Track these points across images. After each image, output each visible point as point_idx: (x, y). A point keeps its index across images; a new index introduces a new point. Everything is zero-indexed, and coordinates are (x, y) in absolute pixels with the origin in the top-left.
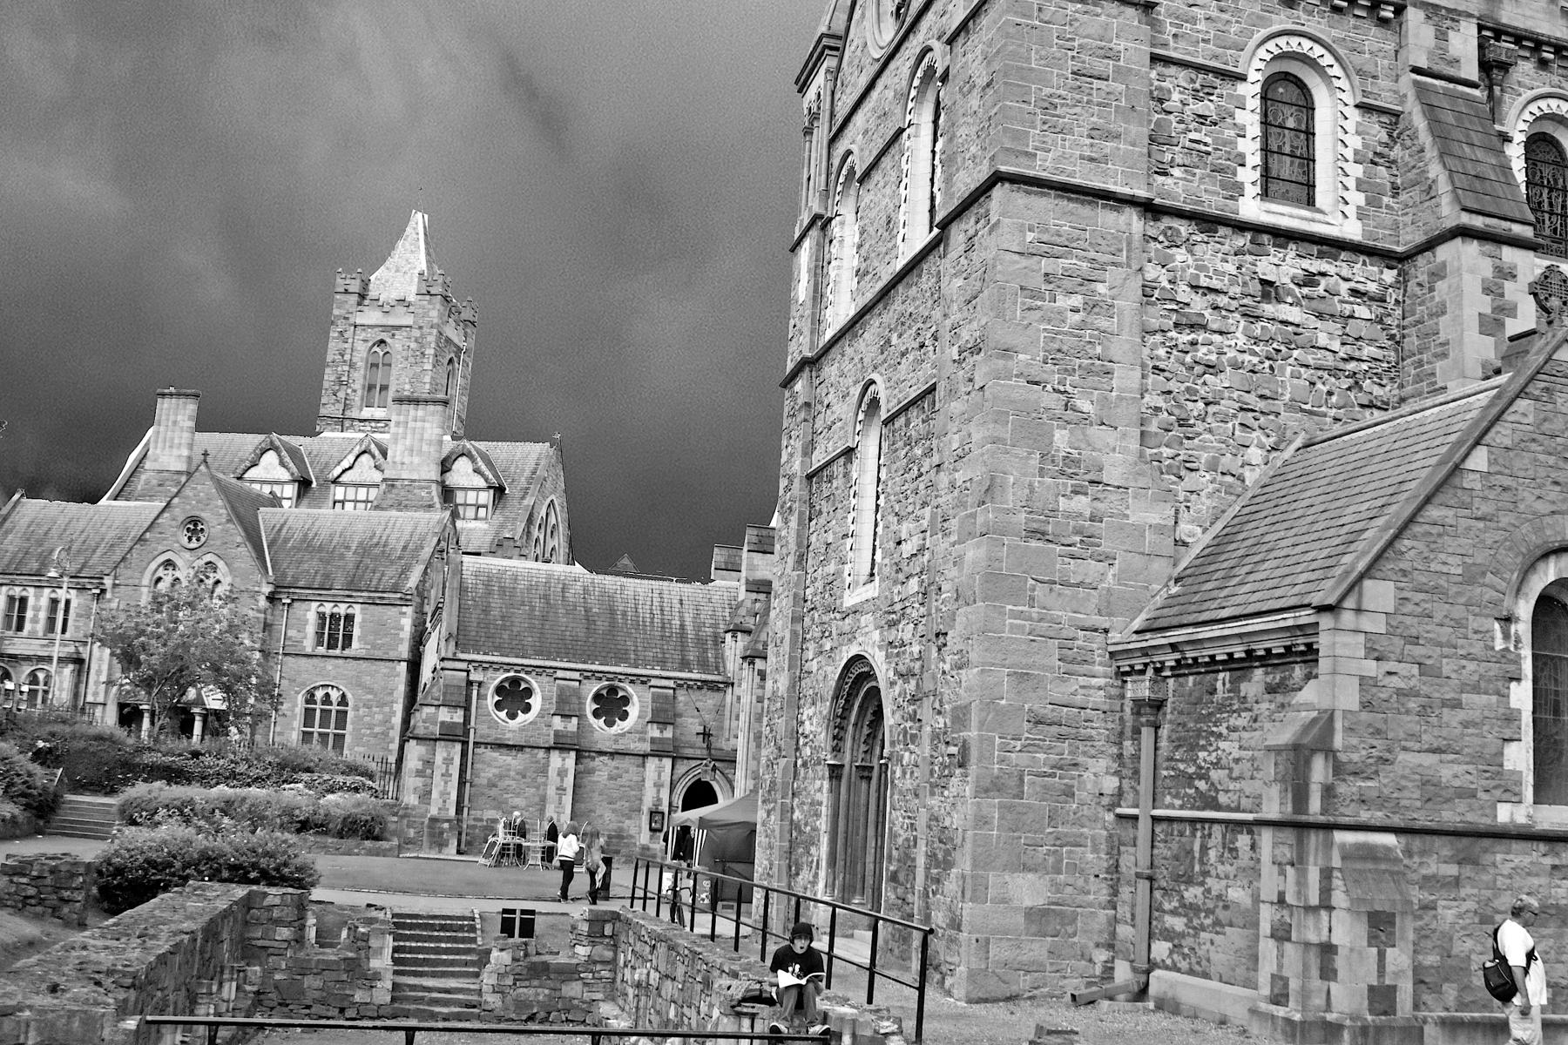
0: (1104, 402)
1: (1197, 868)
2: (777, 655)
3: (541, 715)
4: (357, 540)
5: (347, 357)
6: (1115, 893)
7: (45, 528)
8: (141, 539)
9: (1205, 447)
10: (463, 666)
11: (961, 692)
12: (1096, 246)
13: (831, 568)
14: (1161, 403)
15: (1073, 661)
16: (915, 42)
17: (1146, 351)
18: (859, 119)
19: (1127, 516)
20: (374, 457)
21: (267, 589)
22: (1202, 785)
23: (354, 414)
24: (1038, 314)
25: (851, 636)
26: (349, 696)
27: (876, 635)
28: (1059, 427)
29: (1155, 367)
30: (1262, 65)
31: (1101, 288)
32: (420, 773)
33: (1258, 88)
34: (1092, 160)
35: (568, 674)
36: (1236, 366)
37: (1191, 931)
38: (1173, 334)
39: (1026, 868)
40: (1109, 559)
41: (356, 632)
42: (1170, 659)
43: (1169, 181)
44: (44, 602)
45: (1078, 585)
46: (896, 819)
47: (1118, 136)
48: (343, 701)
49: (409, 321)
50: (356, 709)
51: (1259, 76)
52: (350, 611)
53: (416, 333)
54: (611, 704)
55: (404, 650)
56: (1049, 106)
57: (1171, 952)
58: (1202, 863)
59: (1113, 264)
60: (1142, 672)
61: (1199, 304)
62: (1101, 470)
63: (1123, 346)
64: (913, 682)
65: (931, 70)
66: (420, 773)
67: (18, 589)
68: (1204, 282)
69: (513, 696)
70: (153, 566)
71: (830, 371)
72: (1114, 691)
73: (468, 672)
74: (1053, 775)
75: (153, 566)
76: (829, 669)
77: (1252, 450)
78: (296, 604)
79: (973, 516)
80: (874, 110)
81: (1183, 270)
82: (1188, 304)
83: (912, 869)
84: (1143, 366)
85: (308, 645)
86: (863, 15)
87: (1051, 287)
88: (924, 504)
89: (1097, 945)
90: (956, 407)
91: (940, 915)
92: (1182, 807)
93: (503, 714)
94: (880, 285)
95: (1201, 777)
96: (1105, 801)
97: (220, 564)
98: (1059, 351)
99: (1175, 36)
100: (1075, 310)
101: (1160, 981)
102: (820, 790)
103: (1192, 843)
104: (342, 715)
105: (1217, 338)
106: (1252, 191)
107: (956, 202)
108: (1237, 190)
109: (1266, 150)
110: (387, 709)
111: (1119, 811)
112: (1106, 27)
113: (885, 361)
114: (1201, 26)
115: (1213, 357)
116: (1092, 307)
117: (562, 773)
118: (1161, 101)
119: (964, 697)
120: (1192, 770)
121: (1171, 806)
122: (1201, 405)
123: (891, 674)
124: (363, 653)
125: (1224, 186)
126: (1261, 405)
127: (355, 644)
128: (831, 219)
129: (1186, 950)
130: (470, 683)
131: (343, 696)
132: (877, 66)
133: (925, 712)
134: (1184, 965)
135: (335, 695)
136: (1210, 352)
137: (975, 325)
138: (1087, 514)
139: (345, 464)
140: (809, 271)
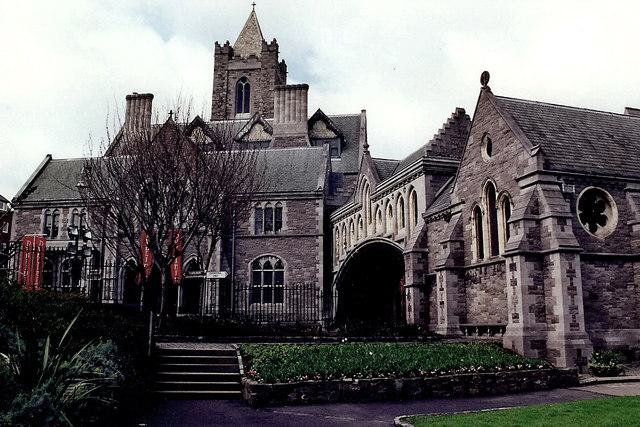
5: (225, 87)
20: (263, 124)
26: (284, 261)
41: (285, 219)
44: (69, 216)
48: (279, 265)
49: (259, 65)
50: (290, 269)
52: (279, 206)
53: (263, 72)
55: (320, 228)
73: (560, 185)
104: (280, 276)
124: (291, 232)
127: (284, 227)
131: (280, 262)
135: (273, 262)
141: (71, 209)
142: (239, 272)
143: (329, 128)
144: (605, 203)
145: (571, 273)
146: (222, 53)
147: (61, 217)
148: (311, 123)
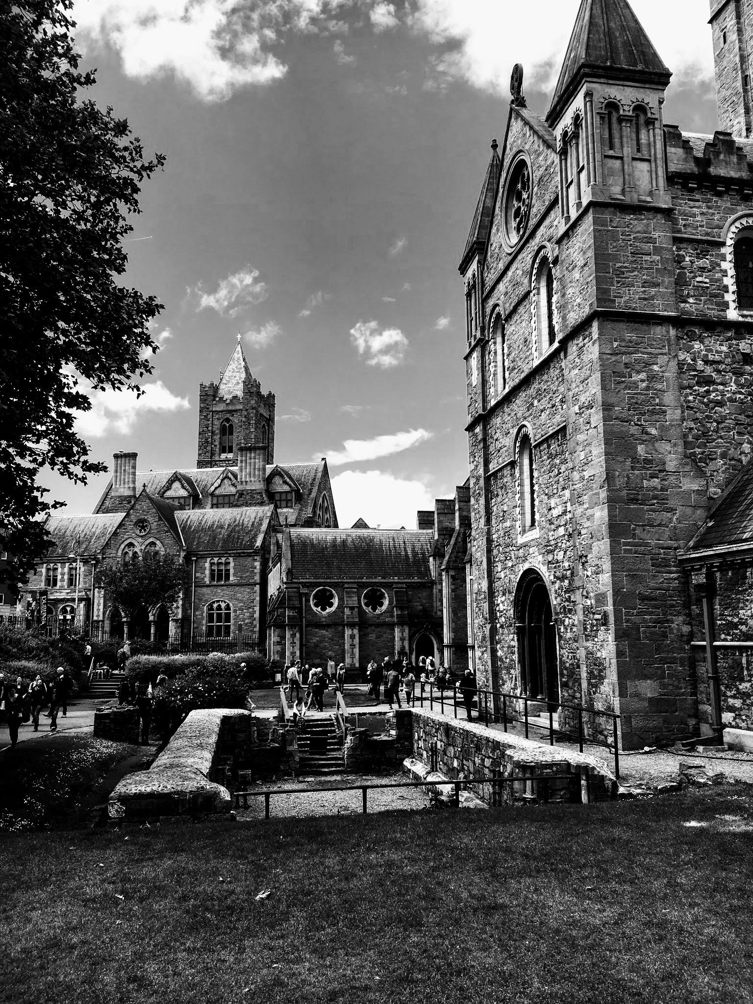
0: (662, 428)
1: (745, 673)
2: (479, 570)
3: (338, 608)
4: (227, 523)
5: (210, 428)
6: (695, 687)
7: (63, 531)
8: (115, 534)
9: (718, 446)
10: (295, 585)
11: (600, 586)
12: (651, 346)
13: (508, 524)
14: (693, 426)
15: (661, 564)
16: (533, 244)
17: (682, 399)
18: (501, 287)
19: (681, 487)
21: (183, 554)
22: (743, 628)
23: (217, 458)
24: (623, 385)
25: (525, 560)
26: (231, 605)
27: (540, 558)
28: (640, 444)
29: (688, 407)
30: (733, 236)
31: (656, 368)
32: (279, 643)
33: (731, 249)
34: (645, 299)
35: (350, 586)
36: (731, 400)
37: (746, 707)
38: (696, 388)
39: (646, 677)
40: (672, 510)
42: (716, 562)
43: (688, 305)
44: (66, 570)
45: (660, 525)
46: (563, 653)
47: (658, 285)
48: (228, 607)
49: (241, 407)
50: (235, 611)
51: (732, 242)
53: (245, 413)
54: (375, 600)
55: (257, 578)
56: (619, 273)
57: (735, 719)
58: (748, 669)
59: (662, 354)
60: (700, 569)
61: (709, 370)
62: (664, 464)
63: (669, 398)
64: (567, 582)
65: (545, 259)
66: (279, 643)
67: (52, 565)
68: (711, 357)
69: (324, 600)
70: (123, 546)
71: (497, 421)
72: (683, 580)
74: (655, 627)
75: (123, 546)
76: (512, 576)
77: (745, 445)
78: (199, 560)
79: (598, 494)
80: (510, 281)
81: (699, 353)
82: (703, 371)
83: (578, 681)
84: (682, 406)
85: (207, 580)
86: (498, 230)
87: (629, 370)
88: (564, 489)
89: (689, 716)
90: (581, 437)
91: (600, 704)
92: (732, 640)
93: (319, 609)
94: (523, 375)
95: (742, 624)
96: (685, 639)
97: (158, 542)
98: (636, 403)
99: (685, 225)
100: (642, 381)
101: (729, 735)
102: (513, 640)
103: (741, 659)
104: (228, 616)
105: (721, 387)
106: (732, 305)
107: (569, 329)
108: (726, 305)
109: (738, 283)
110: (251, 610)
111: (692, 643)
112: (648, 225)
113: (531, 414)
114: (699, 218)
115: (719, 398)
116: (652, 378)
117: (352, 637)
118: (679, 262)
119: (603, 589)
120: (736, 620)
121: (725, 640)
122: (715, 424)
123: (552, 577)
125: (717, 304)
126: (748, 420)
127: (231, 578)
128: (488, 341)
129: (744, 717)
130: (301, 595)
131: (228, 605)
132: (510, 258)
133: (577, 597)
134: (743, 725)
135: (223, 605)
136: (717, 395)
137: (588, 394)
138: (659, 487)
139: (216, 485)
140: (478, 369)
141: (67, 565)
142: (197, 613)
143: (285, 482)
144: (332, 596)
145: (293, 636)
146: (207, 395)
147: (60, 570)
148: (269, 480)
